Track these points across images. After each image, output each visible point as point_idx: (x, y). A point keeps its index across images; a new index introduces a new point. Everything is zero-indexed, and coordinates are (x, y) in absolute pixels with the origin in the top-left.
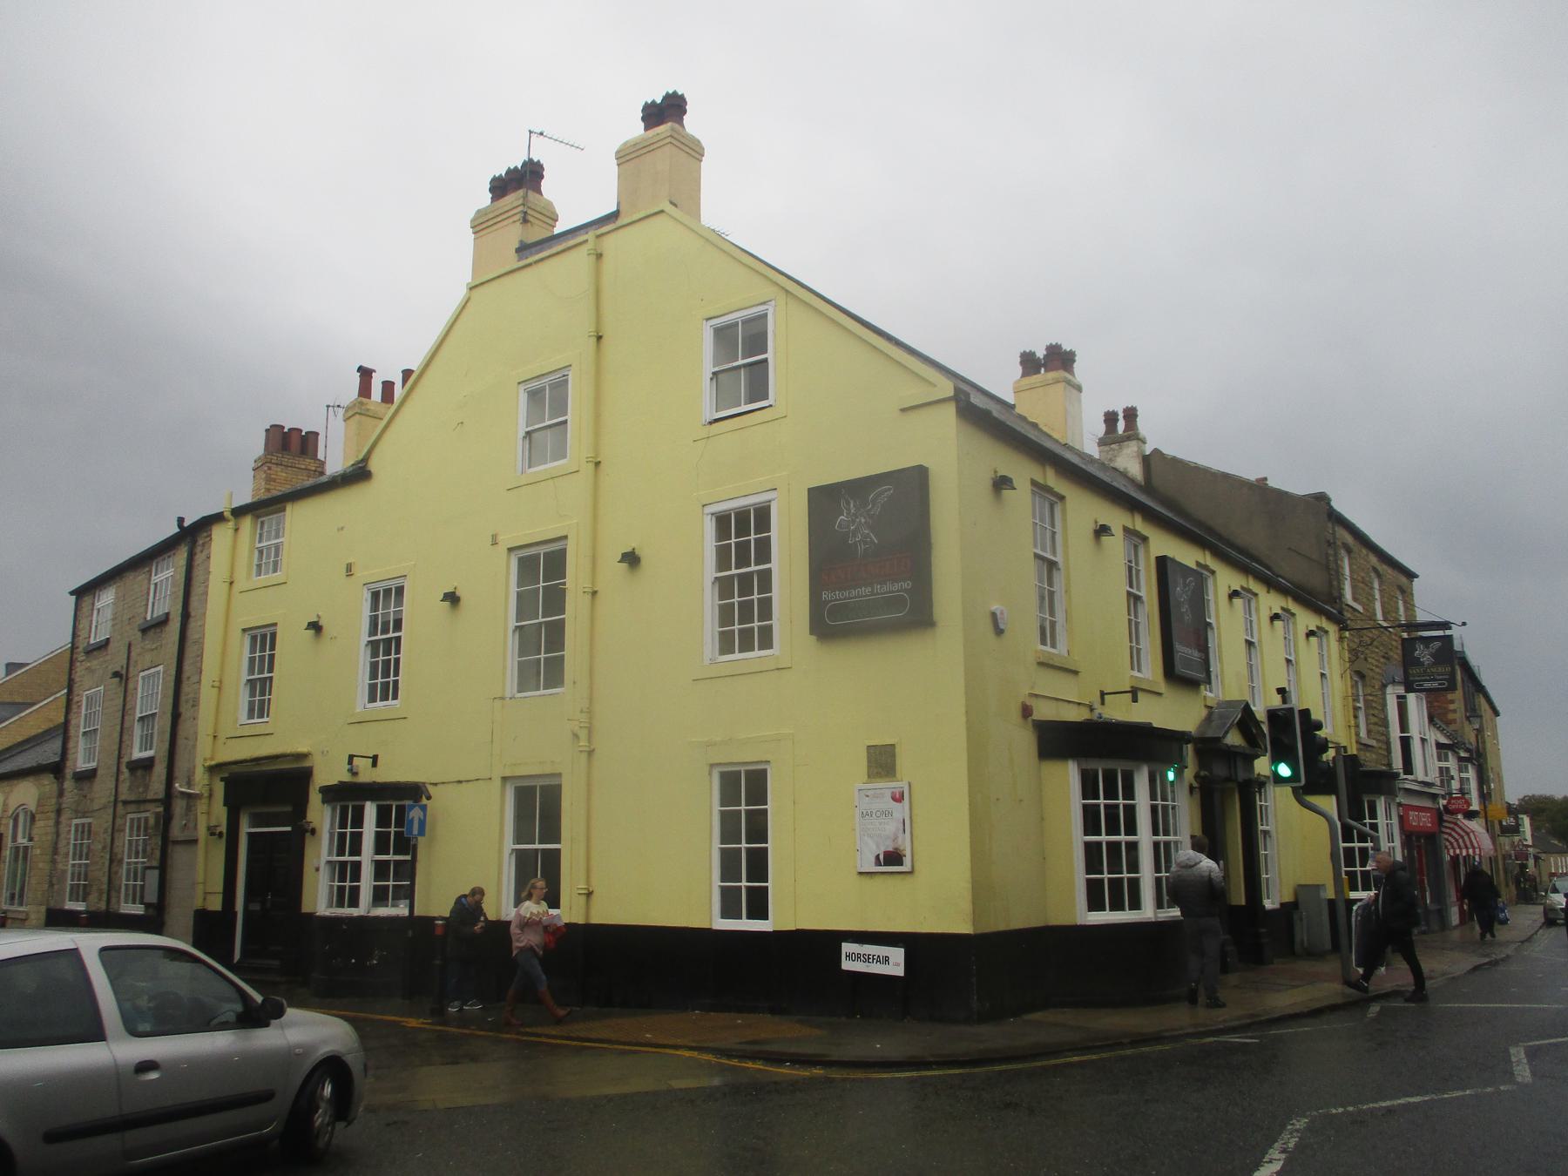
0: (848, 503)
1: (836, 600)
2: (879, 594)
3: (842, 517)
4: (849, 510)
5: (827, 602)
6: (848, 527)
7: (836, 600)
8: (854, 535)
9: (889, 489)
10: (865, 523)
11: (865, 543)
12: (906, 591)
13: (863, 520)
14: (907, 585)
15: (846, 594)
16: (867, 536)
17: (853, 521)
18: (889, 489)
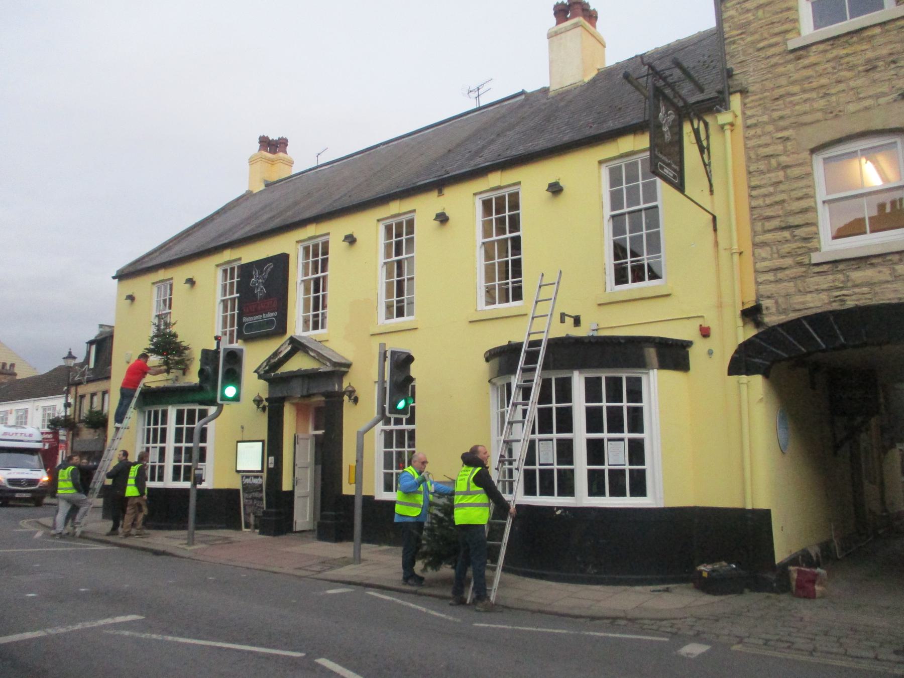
0: (256, 272)
1: (249, 322)
2: (264, 319)
3: (253, 279)
4: (256, 276)
5: (245, 323)
6: (255, 285)
7: (249, 322)
8: (257, 289)
9: (270, 266)
10: (262, 282)
11: (261, 292)
12: (275, 317)
13: (261, 281)
14: (275, 314)
15: (252, 318)
16: (262, 289)
17: (257, 281)
18: (270, 266)
